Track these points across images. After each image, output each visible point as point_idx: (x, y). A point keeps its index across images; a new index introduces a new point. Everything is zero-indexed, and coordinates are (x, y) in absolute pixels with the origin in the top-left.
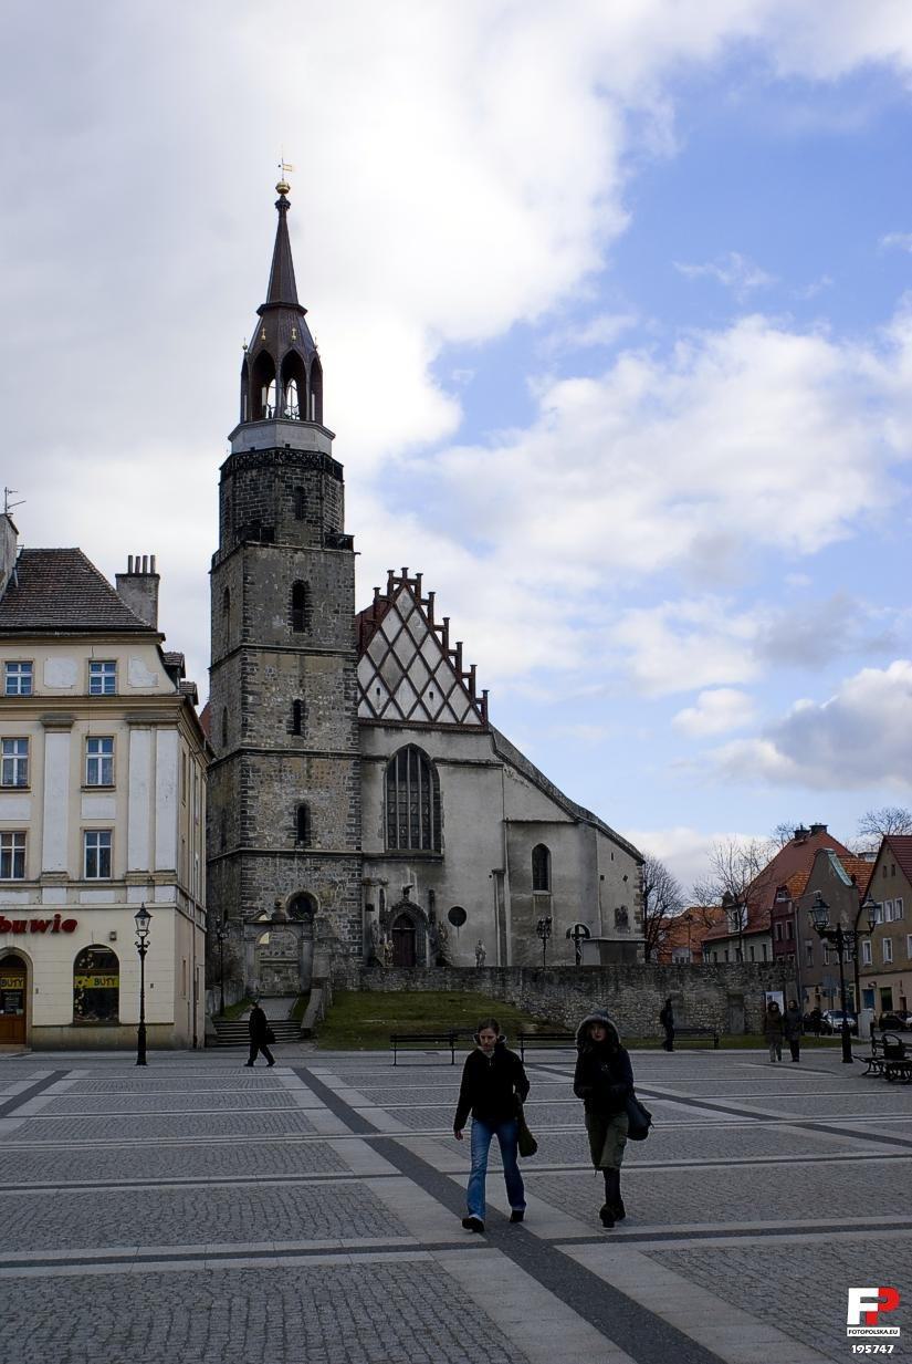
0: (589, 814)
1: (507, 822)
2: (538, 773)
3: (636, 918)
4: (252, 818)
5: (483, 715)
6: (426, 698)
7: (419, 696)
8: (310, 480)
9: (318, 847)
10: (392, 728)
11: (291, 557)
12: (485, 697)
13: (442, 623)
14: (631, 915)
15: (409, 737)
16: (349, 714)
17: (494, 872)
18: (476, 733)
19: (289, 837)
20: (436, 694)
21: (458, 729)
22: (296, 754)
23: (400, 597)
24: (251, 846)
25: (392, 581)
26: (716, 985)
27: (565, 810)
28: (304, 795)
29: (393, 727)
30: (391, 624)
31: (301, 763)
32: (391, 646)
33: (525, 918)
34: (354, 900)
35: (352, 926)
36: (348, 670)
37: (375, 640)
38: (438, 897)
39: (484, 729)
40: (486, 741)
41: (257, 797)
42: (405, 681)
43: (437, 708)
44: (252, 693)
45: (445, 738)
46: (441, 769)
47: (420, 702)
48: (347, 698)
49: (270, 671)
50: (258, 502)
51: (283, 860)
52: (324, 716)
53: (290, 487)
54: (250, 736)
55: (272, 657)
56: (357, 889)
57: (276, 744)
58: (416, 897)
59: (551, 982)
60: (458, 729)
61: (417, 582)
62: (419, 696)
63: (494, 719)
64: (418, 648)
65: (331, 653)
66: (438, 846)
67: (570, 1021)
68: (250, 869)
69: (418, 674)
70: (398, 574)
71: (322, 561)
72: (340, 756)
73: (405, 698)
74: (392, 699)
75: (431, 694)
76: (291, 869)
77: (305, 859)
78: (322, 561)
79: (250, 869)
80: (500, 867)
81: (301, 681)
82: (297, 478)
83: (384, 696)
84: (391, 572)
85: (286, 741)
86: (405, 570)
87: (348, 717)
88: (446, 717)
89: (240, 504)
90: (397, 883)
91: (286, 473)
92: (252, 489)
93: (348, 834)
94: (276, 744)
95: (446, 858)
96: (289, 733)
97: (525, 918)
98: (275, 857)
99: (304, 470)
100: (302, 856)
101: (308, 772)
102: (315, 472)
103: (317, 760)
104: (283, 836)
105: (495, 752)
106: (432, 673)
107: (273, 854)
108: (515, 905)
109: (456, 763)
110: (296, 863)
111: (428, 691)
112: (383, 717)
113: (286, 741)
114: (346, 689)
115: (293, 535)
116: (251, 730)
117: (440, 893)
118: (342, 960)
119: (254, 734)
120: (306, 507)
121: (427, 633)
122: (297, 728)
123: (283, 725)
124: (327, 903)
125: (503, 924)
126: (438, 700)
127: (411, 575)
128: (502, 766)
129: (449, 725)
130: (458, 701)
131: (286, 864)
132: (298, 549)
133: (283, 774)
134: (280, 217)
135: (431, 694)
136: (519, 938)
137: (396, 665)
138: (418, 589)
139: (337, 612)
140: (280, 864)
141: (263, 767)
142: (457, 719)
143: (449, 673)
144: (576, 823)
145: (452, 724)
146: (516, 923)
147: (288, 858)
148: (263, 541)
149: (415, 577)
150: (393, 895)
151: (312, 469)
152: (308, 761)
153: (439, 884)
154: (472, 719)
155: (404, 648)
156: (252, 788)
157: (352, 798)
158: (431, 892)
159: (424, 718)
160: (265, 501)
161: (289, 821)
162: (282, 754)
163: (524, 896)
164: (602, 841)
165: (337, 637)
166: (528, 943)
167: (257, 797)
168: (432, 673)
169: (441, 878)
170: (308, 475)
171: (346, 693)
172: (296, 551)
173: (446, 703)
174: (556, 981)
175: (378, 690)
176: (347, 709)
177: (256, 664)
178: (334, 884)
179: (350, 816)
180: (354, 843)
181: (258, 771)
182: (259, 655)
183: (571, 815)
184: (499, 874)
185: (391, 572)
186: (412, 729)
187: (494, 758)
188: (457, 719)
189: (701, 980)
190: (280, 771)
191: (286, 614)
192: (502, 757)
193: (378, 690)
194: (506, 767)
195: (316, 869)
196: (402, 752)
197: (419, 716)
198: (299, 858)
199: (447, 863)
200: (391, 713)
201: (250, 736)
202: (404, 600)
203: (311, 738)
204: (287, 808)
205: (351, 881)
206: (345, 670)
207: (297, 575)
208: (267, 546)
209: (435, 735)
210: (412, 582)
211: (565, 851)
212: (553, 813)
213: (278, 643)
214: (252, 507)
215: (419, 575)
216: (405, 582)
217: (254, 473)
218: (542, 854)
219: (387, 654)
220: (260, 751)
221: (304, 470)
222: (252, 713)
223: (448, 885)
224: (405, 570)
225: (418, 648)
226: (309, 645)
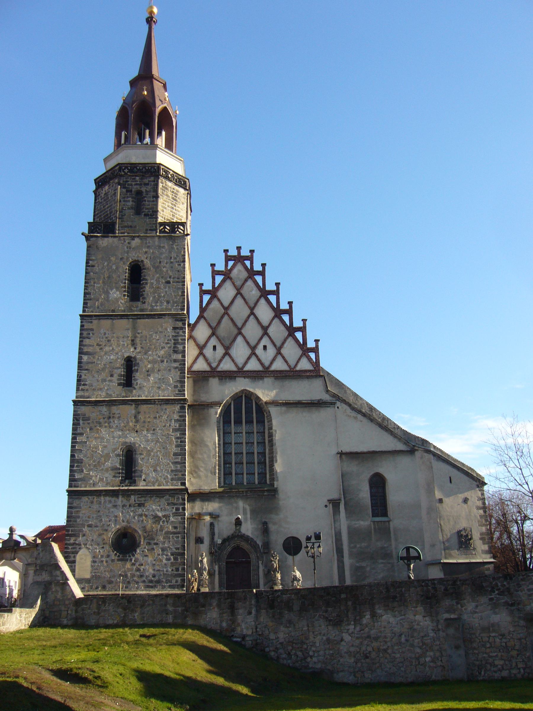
0: (424, 442)
1: (341, 454)
2: (372, 408)
3: (481, 539)
4: (80, 461)
5: (317, 364)
6: (259, 351)
7: (253, 349)
8: (148, 184)
9: (141, 486)
10: (226, 377)
11: (129, 243)
12: (317, 346)
13: (274, 288)
14: (476, 536)
15: (241, 385)
16: (176, 365)
17: (330, 501)
18: (308, 377)
19: (114, 476)
20: (270, 347)
21: (292, 374)
22: (124, 402)
23: (235, 271)
24: (78, 487)
25: (228, 258)
26: (506, 604)
27: (400, 439)
28: (132, 438)
29: (227, 376)
30: (227, 293)
31: (130, 410)
32: (226, 309)
33: (363, 545)
34: (179, 533)
35: (175, 559)
36: (177, 328)
37: (212, 306)
38: (272, 527)
39: (317, 372)
40: (318, 383)
41: (86, 442)
42: (240, 339)
43: (270, 358)
44: (87, 353)
45: (278, 383)
46: (273, 411)
47: (253, 353)
48: (175, 352)
49: (105, 334)
50: (108, 208)
51: (108, 498)
52: (153, 369)
53: (131, 191)
54: (82, 390)
55: (107, 323)
56: (180, 523)
57: (108, 395)
58: (248, 528)
59: (290, 609)
60: (292, 374)
61: (250, 258)
62: (253, 349)
63: (324, 364)
64: (252, 309)
65: (160, 316)
66: (272, 479)
67: (315, 659)
68: (76, 508)
69: (252, 331)
70: (233, 252)
71: (157, 243)
72: (167, 402)
73: (240, 351)
74: (227, 354)
75: (265, 347)
76: (115, 506)
77: (129, 496)
78: (157, 243)
79: (76, 508)
80: (335, 495)
81: (132, 341)
82: (136, 184)
83: (220, 351)
84: (226, 251)
85: (117, 392)
86: (239, 248)
87: (176, 368)
88: (279, 365)
89: (98, 214)
90: (237, 516)
91: (127, 181)
92: (104, 200)
93: (172, 471)
94: (108, 395)
95: (280, 491)
96: (119, 384)
97: (363, 545)
98: (100, 495)
99: (143, 177)
100: (127, 494)
101: (135, 417)
102: (152, 179)
103: (145, 406)
104: (109, 476)
105: (327, 391)
106: (265, 330)
107: (98, 493)
108: (353, 533)
109: (288, 404)
110: (120, 501)
111: (261, 346)
112: (219, 369)
113: (117, 392)
114: (175, 344)
115: (131, 227)
116: (84, 385)
117: (275, 524)
118: (58, 589)
119: (86, 387)
120: (144, 205)
121: (260, 297)
122: (128, 381)
123: (115, 378)
124: (150, 537)
125: (340, 551)
126: (271, 351)
127: (245, 252)
128: (334, 404)
129: (281, 372)
130: (291, 351)
131: (110, 502)
132: (134, 237)
133: (111, 420)
134: (149, 28)
135: (265, 347)
136: (357, 565)
137: (231, 324)
138: (252, 263)
139: (168, 282)
140: (105, 502)
141: (93, 415)
142: (289, 366)
143: (282, 328)
144: (412, 452)
145: (288, 371)
146: (354, 550)
147: (112, 496)
148: (104, 233)
149: (249, 254)
150: (225, 527)
151: (150, 177)
152: (136, 408)
153: (273, 516)
154: (304, 365)
155: (239, 310)
156: (81, 434)
157: (178, 438)
158: (265, 524)
159: (259, 368)
160: (111, 206)
161: (115, 462)
162: (111, 403)
163: (362, 523)
164: (438, 465)
165: (168, 302)
166: (368, 569)
167: (86, 442)
168: (265, 330)
169: (274, 509)
170: (146, 181)
171: (174, 348)
172: (133, 238)
173: (279, 352)
174: (296, 607)
175: (215, 348)
176: (175, 361)
177: (92, 330)
178: (157, 519)
179: (175, 454)
180: (179, 479)
181: (88, 419)
182: (95, 322)
183: (406, 443)
184: (335, 504)
185: (226, 251)
186: (245, 377)
187: (326, 397)
188: (289, 366)
189: (484, 600)
190: (109, 418)
191: (122, 287)
192: (334, 396)
193: (215, 348)
194: (338, 404)
195: (140, 505)
196: (237, 398)
197: (253, 365)
198: (123, 495)
199: (281, 495)
200: (227, 366)
201: (82, 390)
202: (239, 272)
203: (140, 388)
204: (114, 450)
205: (175, 514)
206: (175, 328)
207: (133, 256)
208: (108, 237)
209: (268, 381)
210: (247, 258)
211: (399, 476)
212: (389, 443)
213: (113, 311)
214: (104, 214)
215: (252, 251)
216: (239, 259)
217: (107, 187)
218: (378, 483)
219: (222, 317)
220: (90, 402)
221: (143, 177)
222: (87, 370)
223: (282, 516)
224: (239, 248)
225: (252, 309)
226: (142, 310)
